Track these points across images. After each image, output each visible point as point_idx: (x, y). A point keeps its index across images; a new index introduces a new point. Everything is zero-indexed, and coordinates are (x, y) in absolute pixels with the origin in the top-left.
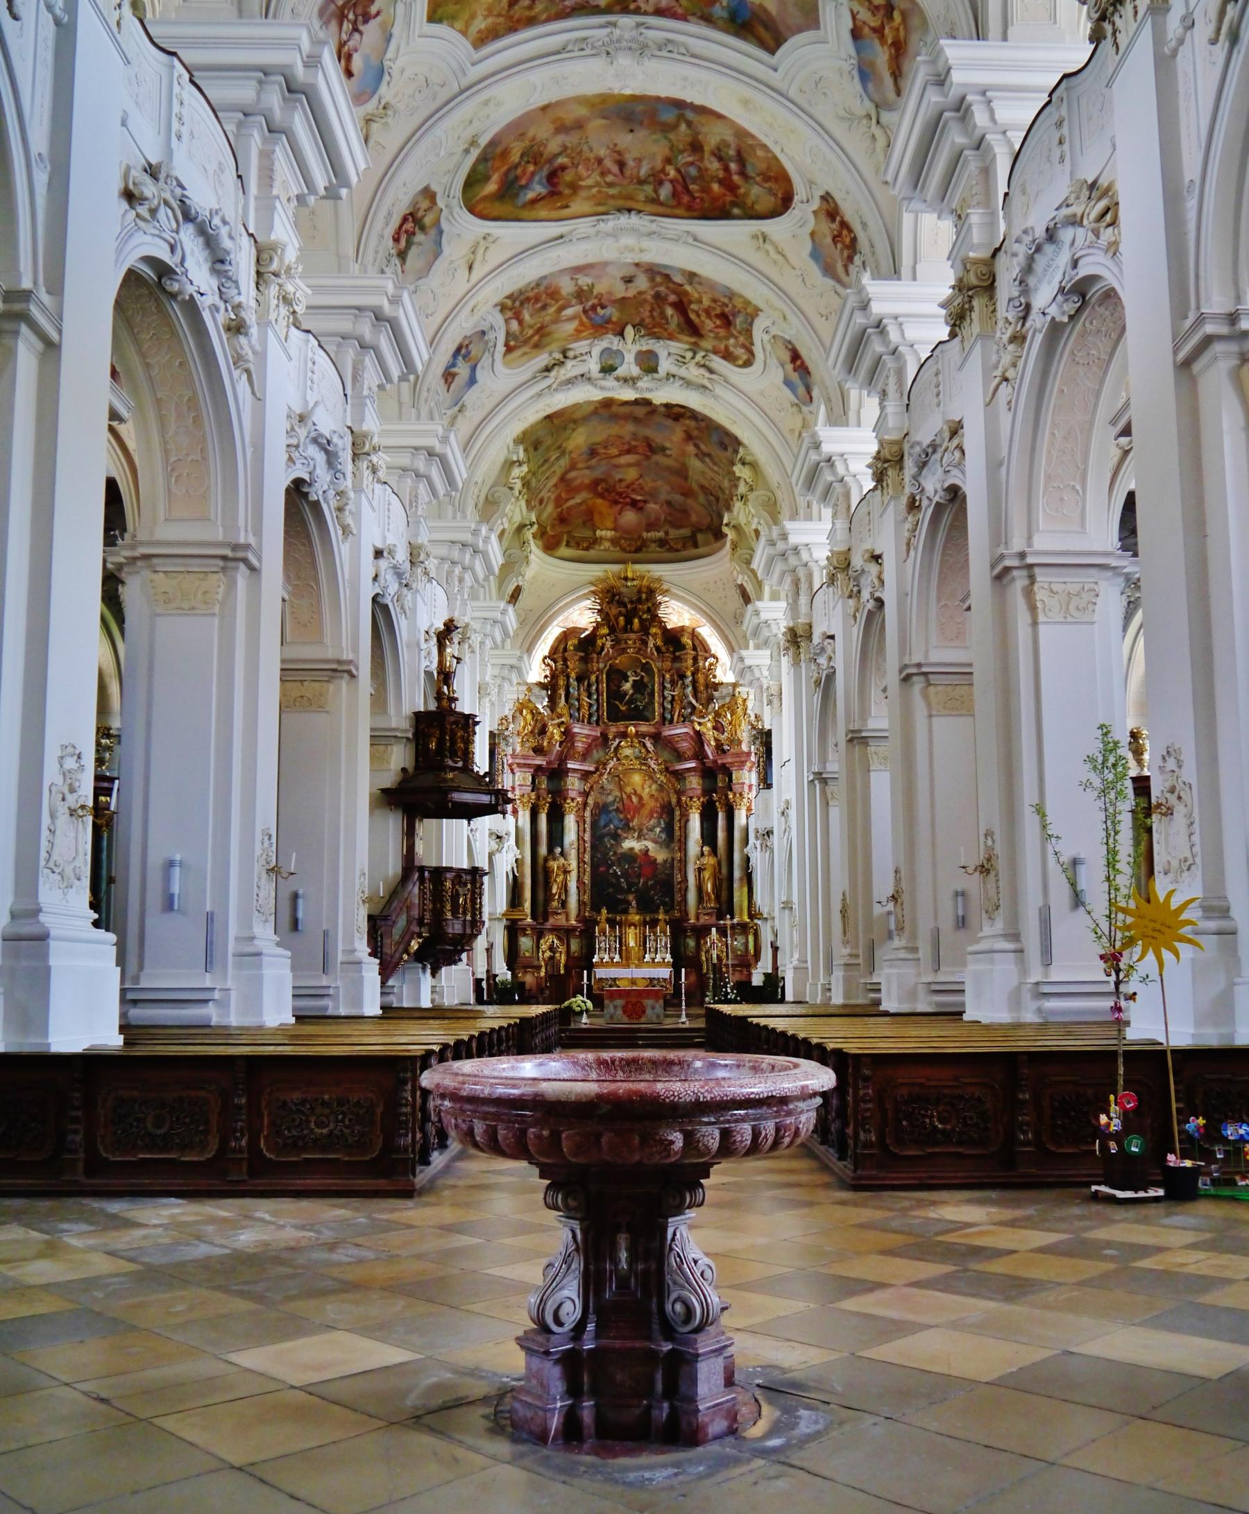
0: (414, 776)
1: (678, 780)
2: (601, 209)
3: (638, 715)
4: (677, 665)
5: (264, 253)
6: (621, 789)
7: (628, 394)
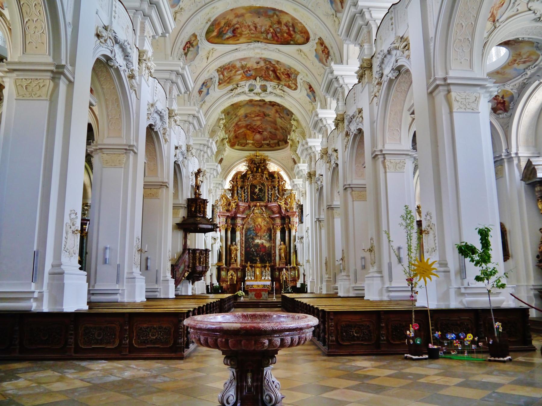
0: (187, 219)
2: (249, 41)
3: (260, 199)
5: (141, 54)
6: (255, 223)
7: (257, 98)
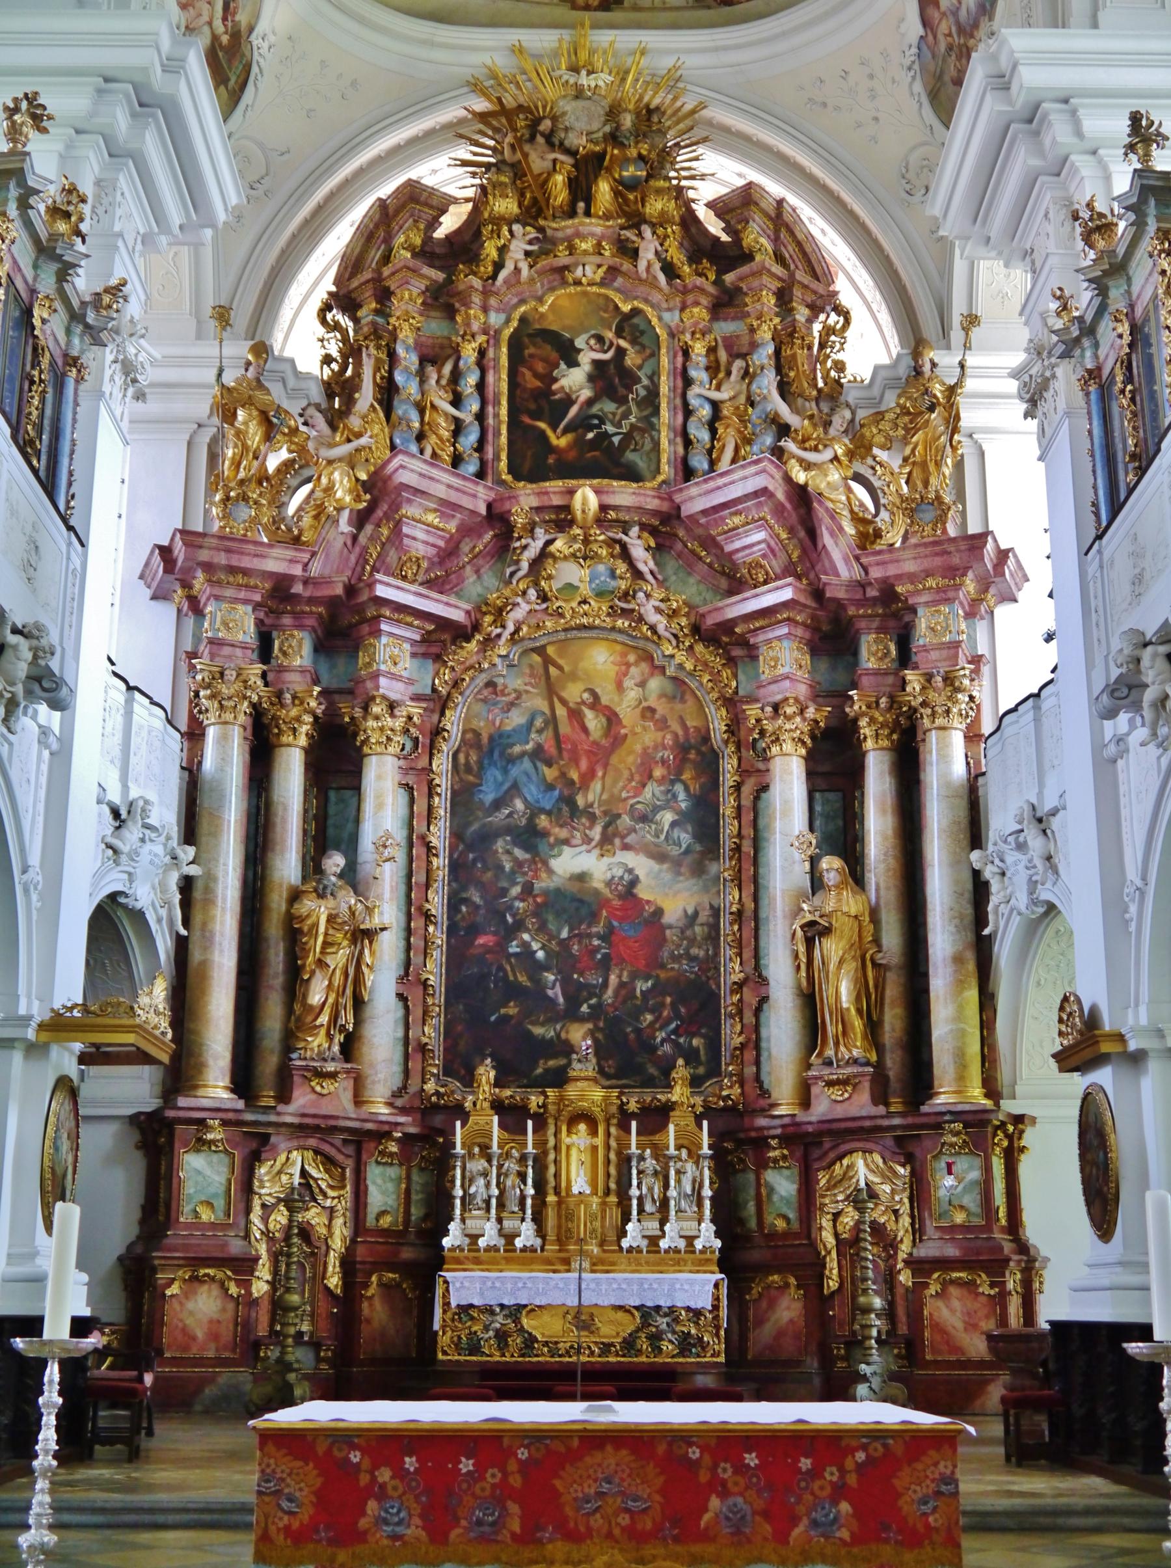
1: (731, 662)
3: (605, 461)
4: (726, 328)
